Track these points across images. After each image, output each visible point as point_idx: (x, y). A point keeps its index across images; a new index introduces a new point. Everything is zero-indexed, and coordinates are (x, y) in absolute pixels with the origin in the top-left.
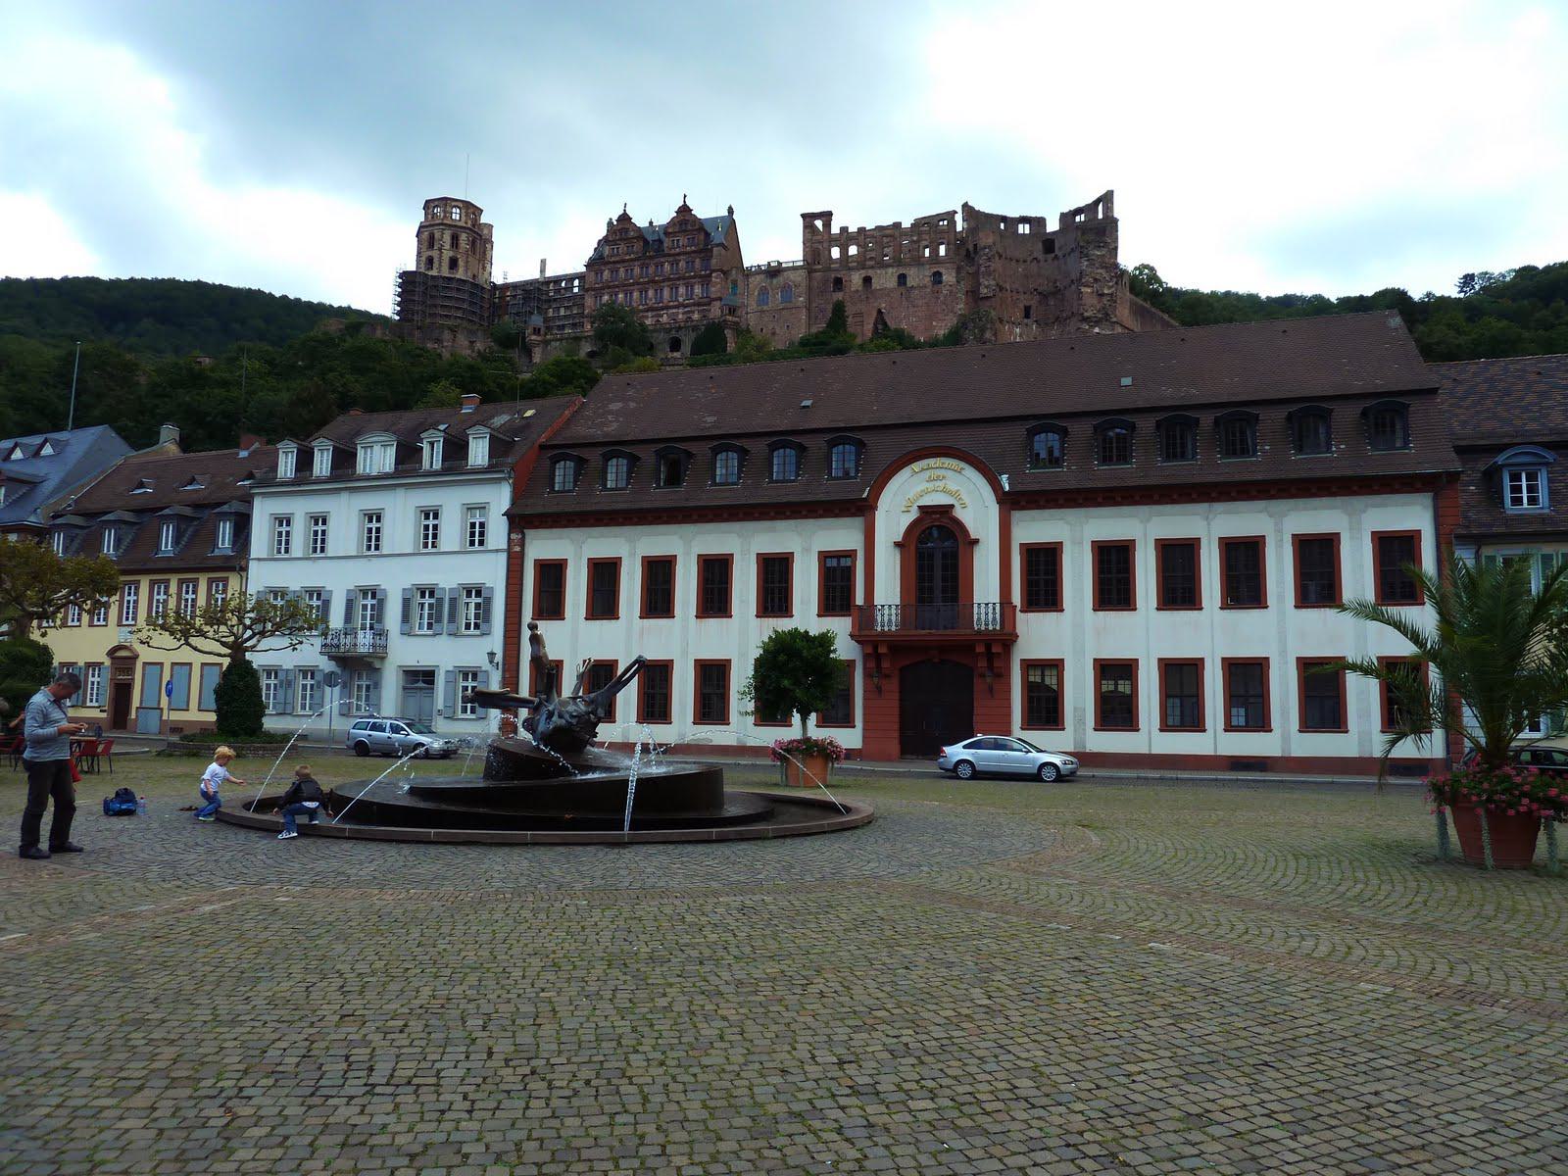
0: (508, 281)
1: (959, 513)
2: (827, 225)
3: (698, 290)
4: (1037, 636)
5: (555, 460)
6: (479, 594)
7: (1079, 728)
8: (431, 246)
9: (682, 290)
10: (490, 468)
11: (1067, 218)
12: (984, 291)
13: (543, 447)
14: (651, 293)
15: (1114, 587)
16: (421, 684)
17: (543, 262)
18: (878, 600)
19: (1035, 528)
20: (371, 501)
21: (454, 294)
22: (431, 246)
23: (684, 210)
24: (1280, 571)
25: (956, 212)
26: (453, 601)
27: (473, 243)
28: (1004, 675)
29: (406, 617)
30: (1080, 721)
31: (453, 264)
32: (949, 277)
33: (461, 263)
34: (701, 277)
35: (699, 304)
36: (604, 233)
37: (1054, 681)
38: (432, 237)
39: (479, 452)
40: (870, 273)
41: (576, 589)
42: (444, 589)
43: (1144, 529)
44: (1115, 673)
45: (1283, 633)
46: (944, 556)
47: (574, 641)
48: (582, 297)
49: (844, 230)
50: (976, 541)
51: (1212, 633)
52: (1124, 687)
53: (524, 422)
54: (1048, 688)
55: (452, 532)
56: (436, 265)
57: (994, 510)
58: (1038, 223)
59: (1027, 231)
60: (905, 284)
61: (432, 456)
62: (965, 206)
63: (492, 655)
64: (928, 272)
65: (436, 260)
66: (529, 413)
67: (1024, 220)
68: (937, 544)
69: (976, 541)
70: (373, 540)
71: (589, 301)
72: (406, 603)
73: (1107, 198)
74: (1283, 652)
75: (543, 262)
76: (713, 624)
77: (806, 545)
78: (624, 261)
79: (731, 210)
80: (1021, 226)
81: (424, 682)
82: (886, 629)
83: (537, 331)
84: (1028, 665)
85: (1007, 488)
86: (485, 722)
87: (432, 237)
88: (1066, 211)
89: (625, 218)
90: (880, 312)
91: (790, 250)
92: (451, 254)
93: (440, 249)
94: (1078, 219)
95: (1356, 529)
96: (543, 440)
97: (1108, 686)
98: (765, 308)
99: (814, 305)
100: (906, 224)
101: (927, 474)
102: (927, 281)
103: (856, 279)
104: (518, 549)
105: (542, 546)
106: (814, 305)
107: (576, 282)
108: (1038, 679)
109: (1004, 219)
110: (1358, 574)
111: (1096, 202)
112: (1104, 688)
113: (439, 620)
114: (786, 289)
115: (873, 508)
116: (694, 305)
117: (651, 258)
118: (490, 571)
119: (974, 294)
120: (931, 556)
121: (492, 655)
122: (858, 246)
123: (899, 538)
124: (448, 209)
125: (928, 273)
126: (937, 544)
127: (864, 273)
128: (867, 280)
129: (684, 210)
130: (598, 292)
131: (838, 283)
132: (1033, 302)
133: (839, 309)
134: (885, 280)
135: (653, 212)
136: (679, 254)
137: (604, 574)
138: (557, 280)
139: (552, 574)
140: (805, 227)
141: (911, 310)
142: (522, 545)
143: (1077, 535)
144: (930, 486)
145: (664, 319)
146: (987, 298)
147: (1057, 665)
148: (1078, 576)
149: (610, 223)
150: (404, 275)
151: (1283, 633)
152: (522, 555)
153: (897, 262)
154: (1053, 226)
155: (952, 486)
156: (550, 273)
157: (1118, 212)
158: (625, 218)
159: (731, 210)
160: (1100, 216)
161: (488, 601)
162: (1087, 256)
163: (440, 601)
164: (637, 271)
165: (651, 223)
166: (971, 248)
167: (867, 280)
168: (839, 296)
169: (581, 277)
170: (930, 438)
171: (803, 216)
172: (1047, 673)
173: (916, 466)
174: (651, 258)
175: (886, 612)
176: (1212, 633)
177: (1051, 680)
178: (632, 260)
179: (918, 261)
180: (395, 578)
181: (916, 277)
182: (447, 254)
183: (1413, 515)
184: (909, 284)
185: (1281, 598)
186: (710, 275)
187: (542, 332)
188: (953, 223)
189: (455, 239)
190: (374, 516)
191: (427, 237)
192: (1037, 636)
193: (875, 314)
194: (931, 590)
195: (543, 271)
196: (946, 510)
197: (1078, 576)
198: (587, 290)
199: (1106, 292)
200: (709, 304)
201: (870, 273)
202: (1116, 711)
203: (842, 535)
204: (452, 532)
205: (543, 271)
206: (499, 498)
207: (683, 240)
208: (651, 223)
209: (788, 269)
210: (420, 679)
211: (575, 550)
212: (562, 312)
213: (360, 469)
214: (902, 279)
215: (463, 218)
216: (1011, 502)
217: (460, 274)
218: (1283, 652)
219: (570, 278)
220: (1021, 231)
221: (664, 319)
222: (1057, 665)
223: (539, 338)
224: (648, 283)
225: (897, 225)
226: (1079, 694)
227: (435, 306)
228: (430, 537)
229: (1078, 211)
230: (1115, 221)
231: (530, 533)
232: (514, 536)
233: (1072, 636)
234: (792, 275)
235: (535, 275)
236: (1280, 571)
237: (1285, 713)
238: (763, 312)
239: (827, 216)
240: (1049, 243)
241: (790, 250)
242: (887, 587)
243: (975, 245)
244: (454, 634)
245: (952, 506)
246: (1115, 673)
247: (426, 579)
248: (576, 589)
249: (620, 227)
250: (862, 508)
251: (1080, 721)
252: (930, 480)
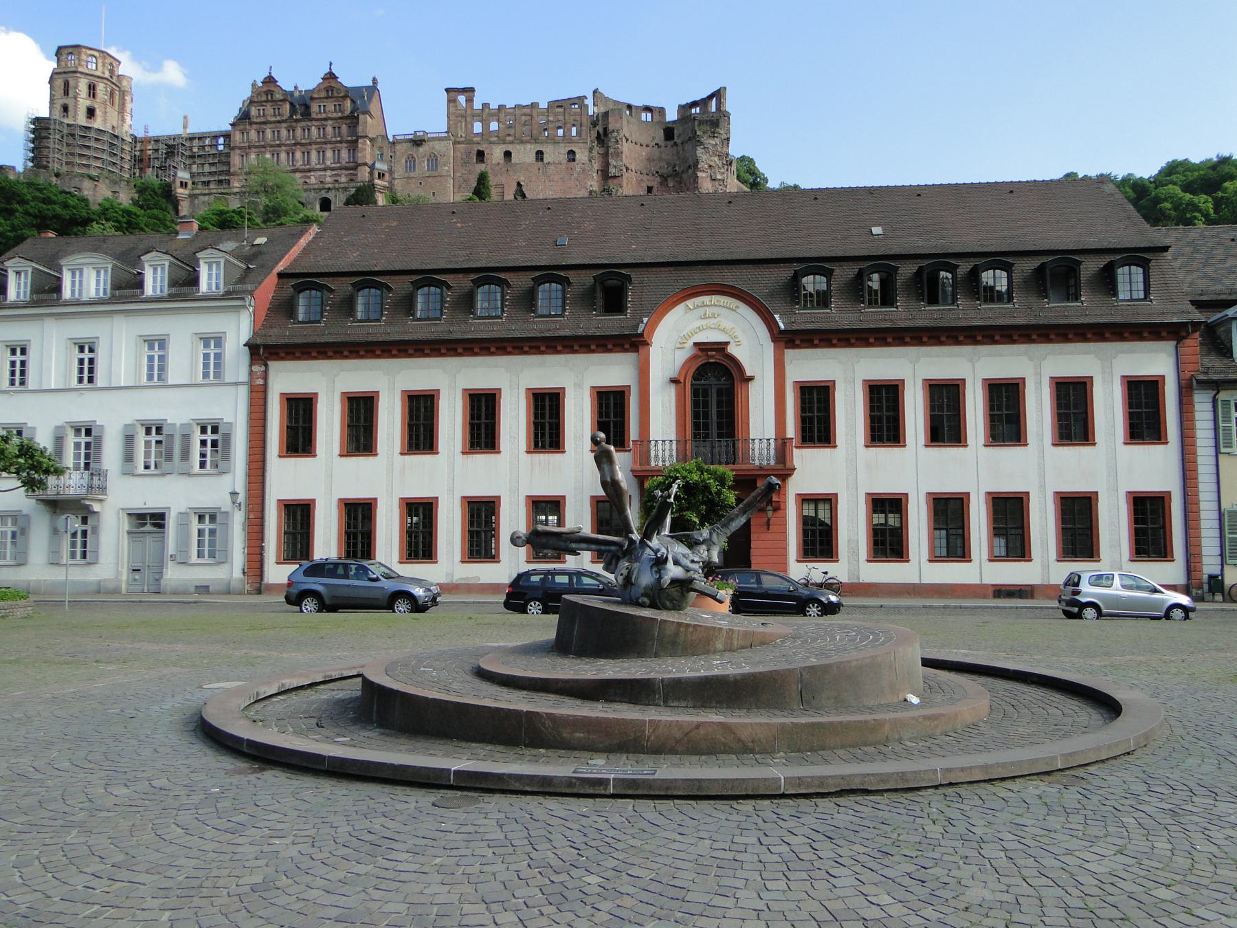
0: (150, 134)
1: (731, 350)
2: (470, 101)
3: (344, 154)
4: (813, 471)
5: (299, 289)
6: (215, 430)
7: (853, 560)
8: (66, 93)
9: (329, 154)
10: (228, 295)
11: (684, 109)
12: (612, 171)
13: (281, 275)
14: (298, 155)
15: (885, 426)
16: (148, 528)
17: (185, 117)
18: (653, 436)
19: (810, 366)
20: (84, 329)
21: (93, 144)
22: (66, 93)
23: (331, 76)
24: (1039, 411)
25: (585, 97)
26: (186, 439)
27: (112, 94)
28: (778, 508)
29: (129, 455)
30: (854, 553)
31: (91, 112)
33: (98, 112)
34: (347, 142)
35: (347, 169)
36: (249, 94)
37: (828, 515)
38: (67, 84)
39: (209, 278)
41: (329, 424)
42: (174, 425)
43: (914, 369)
44: (888, 506)
45: (1041, 469)
46: (720, 393)
47: (324, 478)
48: (228, 155)
49: (485, 106)
50: (751, 379)
51: (977, 469)
52: (893, 520)
53: (254, 249)
54: (822, 523)
55: (183, 359)
56: (71, 113)
57: (769, 347)
58: (662, 111)
59: (649, 119)
60: (542, 160)
61: (154, 279)
62: (595, 92)
63: (234, 494)
64: (564, 149)
65: (71, 108)
66: (261, 240)
67: (648, 109)
68: (714, 384)
69: (751, 379)
70: (87, 372)
71: (236, 160)
72: (129, 441)
73: (718, 94)
74: (1043, 487)
75: (185, 117)
76: (481, 460)
77: (579, 380)
78: (271, 123)
79: (375, 81)
80: (643, 115)
81: (155, 525)
82: (660, 464)
83: (184, 185)
84: (805, 499)
85: (782, 327)
86: (226, 567)
87: (67, 84)
88: (683, 103)
89: (270, 80)
90: (519, 184)
91: (434, 120)
92: (88, 103)
93: (75, 98)
94: (693, 111)
95: (1108, 371)
96: (281, 267)
97: (879, 519)
98: (412, 175)
100: (543, 105)
101: (701, 311)
102: (564, 158)
103: (496, 154)
104: (261, 382)
105: (288, 378)
107: (221, 140)
108: (812, 514)
109: (629, 107)
110: (1108, 409)
111: (710, 97)
112: (875, 521)
113: (169, 458)
114: (433, 160)
115: (647, 344)
116: (340, 168)
117: (297, 121)
118: (231, 408)
119: (605, 175)
120: (706, 393)
121: (234, 494)
122: (498, 121)
123: (674, 375)
124: (84, 57)
126: (714, 384)
127: (505, 148)
128: (508, 154)
129: (331, 76)
130: (245, 150)
131: (481, 155)
132: (655, 182)
133: (482, 179)
134: (524, 154)
135: (300, 77)
136: (325, 119)
137: (360, 411)
138: (201, 138)
139: (301, 411)
140: (449, 101)
142: (265, 378)
143: (849, 374)
144: (704, 322)
145: (313, 180)
146: (615, 177)
147: (830, 500)
148: (850, 414)
149: (254, 85)
150: (37, 121)
151: (1041, 469)
152: (264, 389)
153: (535, 140)
154: (672, 115)
155: (726, 323)
156: (193, 129)
157: (729, 106)
158: (270, 80)
159: (375, 81)
160: (714, 109)
161: (227, 437)
162: (702, 144)
163: (170, 437)
164: (284, 133)
165: (296, 88)
166: (601, 132)
167: (508, 154)
168: (481, 167)
169: (227, 136)
170: (698, 277)
171: (447, 90)
172: (821, 506)
173: (690, 303)
174: (297, 121)
175: (660, 446)
176: (977, 469)
177: (823, 514)
179: (554, 140)
180: (113, 415)
181: (555, 154)
182: (84, 102)
183: (1156, 361)
184: (545, 160)
185: (1041, 436)
186: (356, 141)
187: (190, 185)
188: (584, 107)
189: (92, 88)
190: (86, 347)
191: (62, 82)
192: (813, 471)
193: (515, 185)
194: (706, 426)
195: (185, 127)
196: (721, 347)
197: (850, 414)
198: (233, 149)
199: (719, 177)
200: (355, 168)
201: (510, 148)
202: (888, 543)
203: (613, 371)
204: (183, 359)
205: (185, 127)
206: (238, 328)
207: (330, 107)
208: (296, 88)
209: (433, 139)
210: (150, 521)
211: (328, 384)
212: (207, 169)
213: (67, 293)
214: (540, 155)
215: (100, 68)
216: (787, 339)
217: (98, 123)
218: (1043, 487)
219: (215, 137)
220: (643, 118)
221: (313, 180)
222: (830, 500)
223: (187, 192)
224: (295, 144)
225: (534, 105)
226: (853, 528)
227: (72, 154)
228: (157, 371)
229: (694, 104)
230: (727, 115)
231: (273, 365)
232: (256, 368)
233: (844, 471)
234: (438, 146)
235: (179, 130)
236: (1039, 411)
237: (1045, 545)
238: (409, 178)
239: (469, 91)
240: (669, 132)
241: (434, 120)
242: (662, 421)
243: (605, 129)
244: (187, 474)
245: (727, 343)
246: (888, 506)
247: (153, 415)
248: (329, 424)
249: (265, 89)
250: (634, 343)
251: (854, 553)
252: (705, 317)
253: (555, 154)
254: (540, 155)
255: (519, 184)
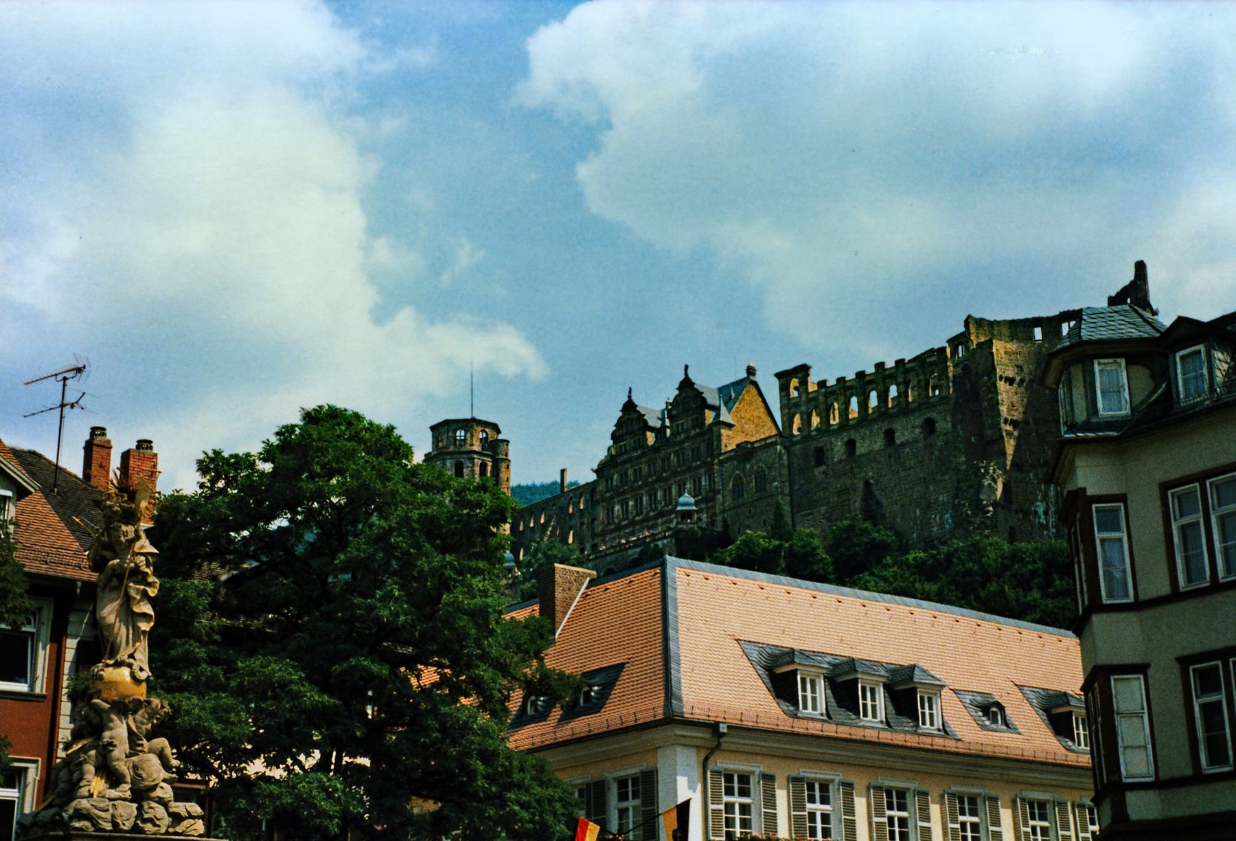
2: (804, 382)
17: (563, 471)
32: (944, 425)
40: (853, 435)
49: (822, 384)
75: (563, 471)
90: (867, 484)
99: (796, 487)
106: (796, 487)
109: (1037, 322)
125: (918, 422)
128: (851, 445)
129: (686, 384)
141: (903, 474)
167: (851, 445)
171: (778, 375)
178: (638, 457)
184: (898, 442)
193: (861, 485)
214: (890, 435)
239: (802, 371)
253: (907, 431)
254: (890, 435)
255: (867, 484)
